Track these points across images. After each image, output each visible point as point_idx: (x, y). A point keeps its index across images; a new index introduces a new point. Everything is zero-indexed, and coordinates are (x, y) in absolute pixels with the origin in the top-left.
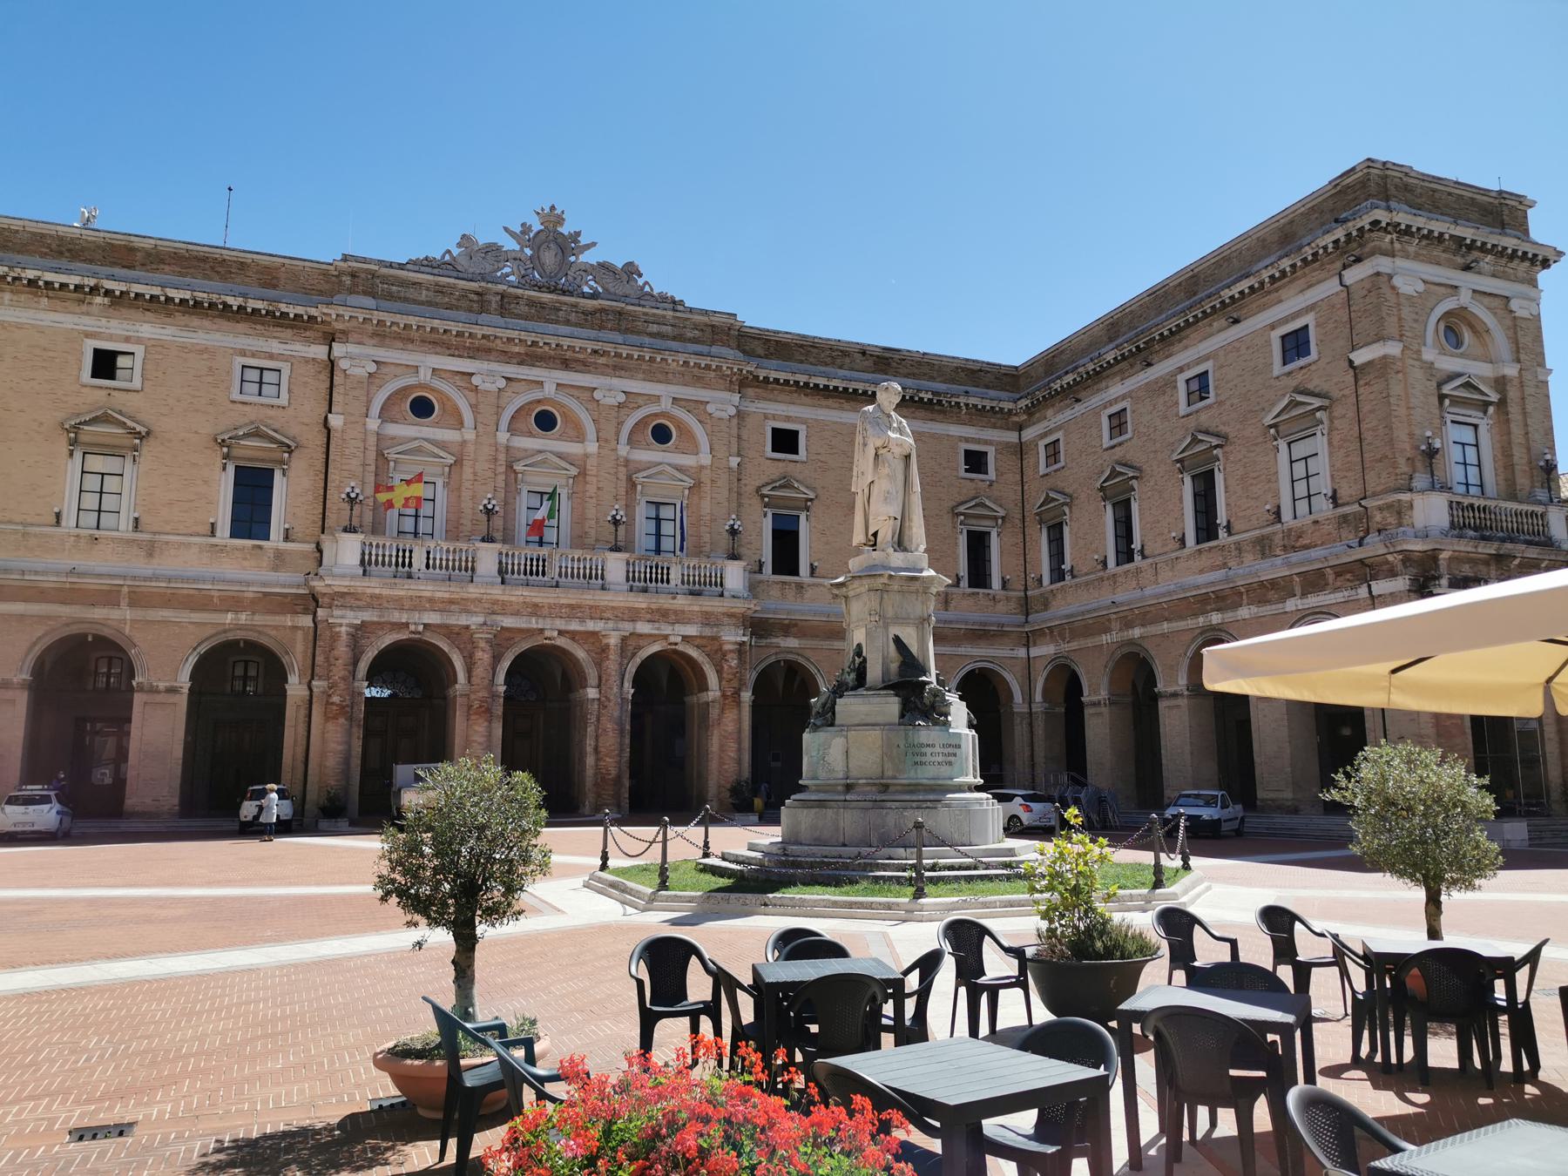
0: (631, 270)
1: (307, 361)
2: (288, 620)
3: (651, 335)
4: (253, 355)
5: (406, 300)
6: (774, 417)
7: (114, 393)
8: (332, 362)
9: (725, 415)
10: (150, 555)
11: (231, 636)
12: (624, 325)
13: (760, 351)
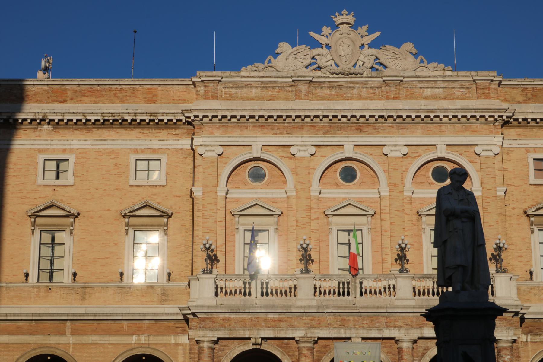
1: (178, 151)
2: (172, 339)
3: (426, 98)
4: (143, 151)
5: (242, 98)
7: (57, 189)
8: (193, 149)
9: (491, 154)
10: (83, 298)
11: (136, 352)
12: (403, 93)
13: (521, 99)
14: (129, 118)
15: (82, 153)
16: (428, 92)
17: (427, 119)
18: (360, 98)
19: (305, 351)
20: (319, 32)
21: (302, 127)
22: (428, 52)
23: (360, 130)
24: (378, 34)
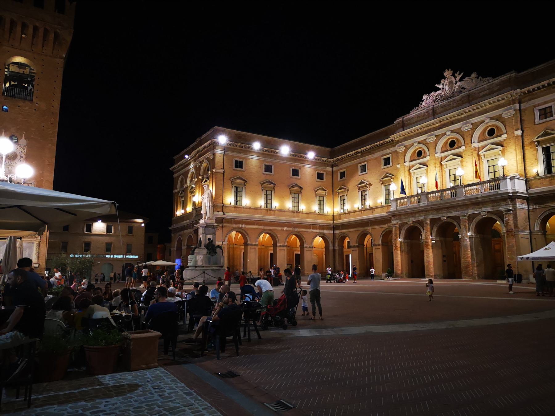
6: (539, 105)
12: (471, 99)
20: (439, 83)
22: (483, 74)
24: (462, 74)
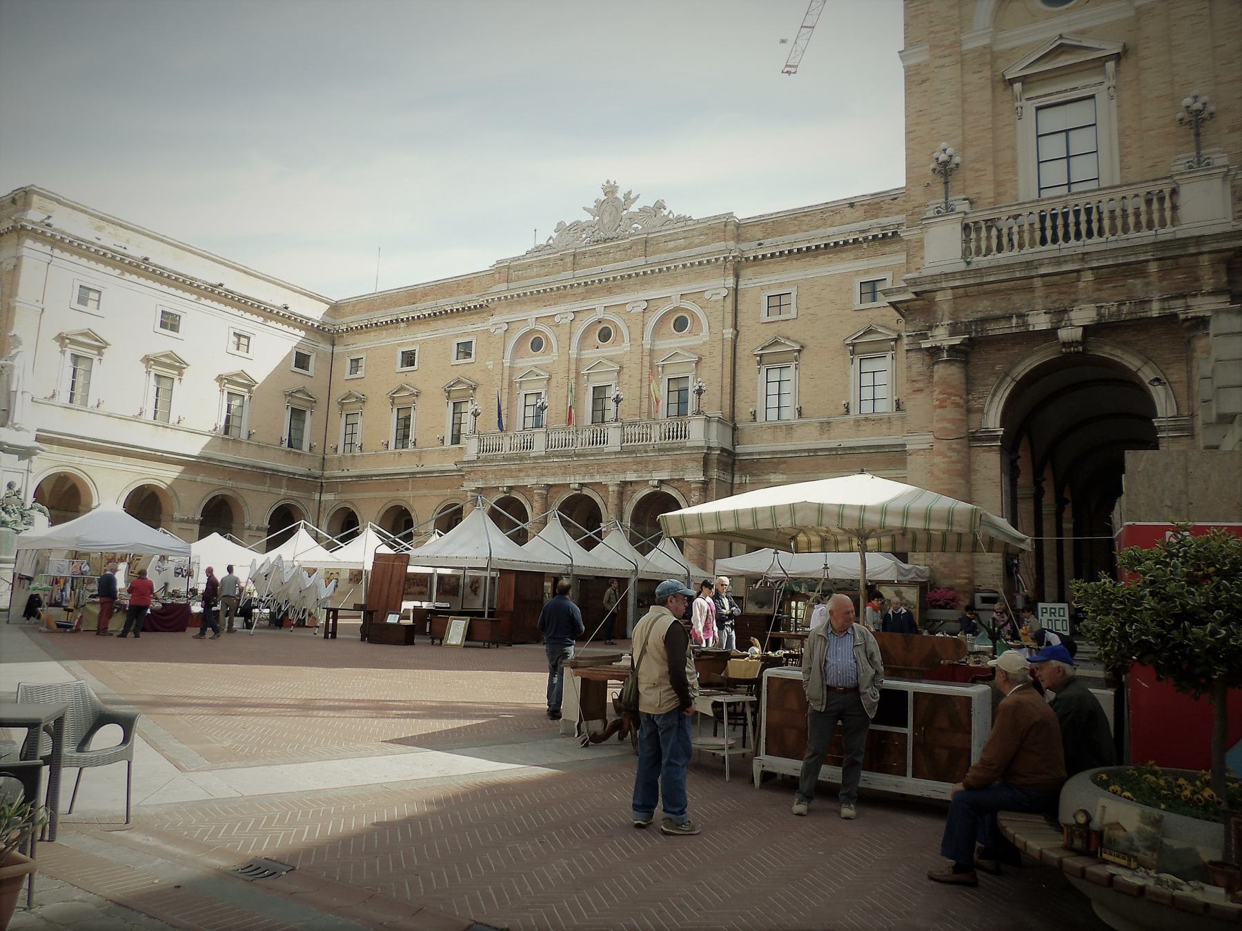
0: (660, 206)
3: (670, 251)
12: (650, 250)
14: (448, 309)
15: (425, 342)
16: (671, 245)
17: (661, 274)
18: (615, 261)
19: (536, 497)
21: (565, 296)
23: (610, 291)
